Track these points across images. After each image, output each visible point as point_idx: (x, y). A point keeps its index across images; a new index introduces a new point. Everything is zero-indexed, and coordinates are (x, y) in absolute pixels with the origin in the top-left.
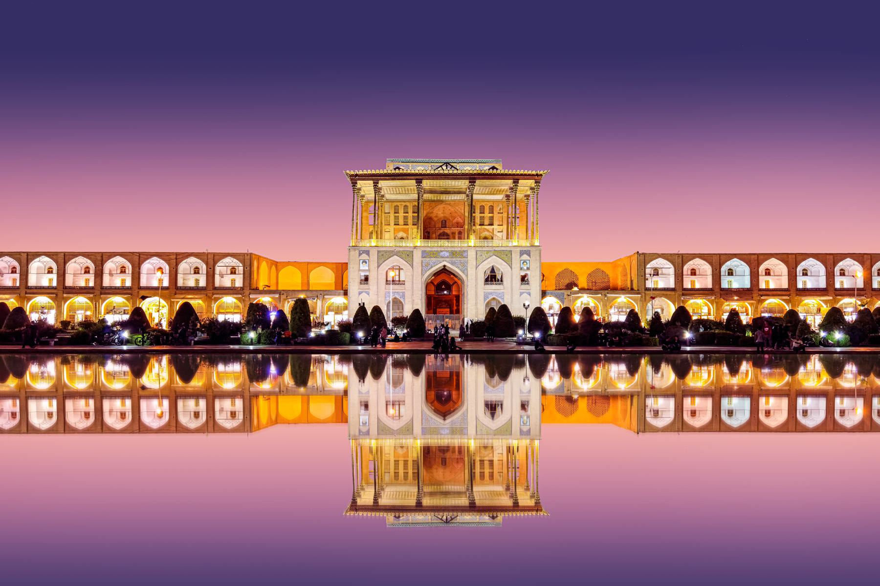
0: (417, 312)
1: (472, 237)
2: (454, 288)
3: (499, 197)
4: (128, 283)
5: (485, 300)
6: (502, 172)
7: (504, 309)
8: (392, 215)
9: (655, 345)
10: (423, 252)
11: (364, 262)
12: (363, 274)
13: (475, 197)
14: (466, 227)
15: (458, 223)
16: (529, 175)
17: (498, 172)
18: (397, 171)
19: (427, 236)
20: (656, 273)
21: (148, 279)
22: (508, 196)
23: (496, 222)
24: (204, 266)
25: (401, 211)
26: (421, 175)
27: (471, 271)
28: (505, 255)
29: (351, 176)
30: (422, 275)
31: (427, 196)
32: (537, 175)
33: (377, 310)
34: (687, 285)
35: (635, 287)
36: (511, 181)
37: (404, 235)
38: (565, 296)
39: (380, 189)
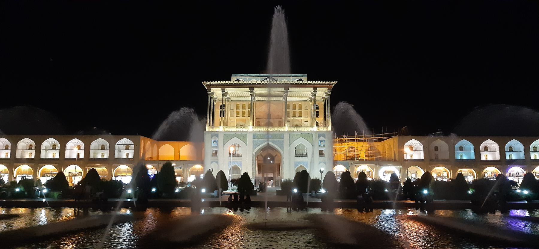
0: (246, 175)
1: (286, 125)
2: (276, 159)
3: (306, 99)
4: (57, 156)
5: (295, 167)
6: (306, 82)
8: (235, 110)
11: (215, 141)
12: (214, 149)
13: (288, 99)
15: (278, 116)
17: (304, 82)
18: (237, 82)
19: (258, 124)
21: (70, 153)
22: (310, 98)
23: (303, 115)
24: (108, 144)
26: (253, 84)
27: (286, 147)
29: (207, 85)
30: (253, 150)
35: (397, 160)
36: (312, 88)
37: (243, 124)
38: (350, 165)
39: (227, 93)
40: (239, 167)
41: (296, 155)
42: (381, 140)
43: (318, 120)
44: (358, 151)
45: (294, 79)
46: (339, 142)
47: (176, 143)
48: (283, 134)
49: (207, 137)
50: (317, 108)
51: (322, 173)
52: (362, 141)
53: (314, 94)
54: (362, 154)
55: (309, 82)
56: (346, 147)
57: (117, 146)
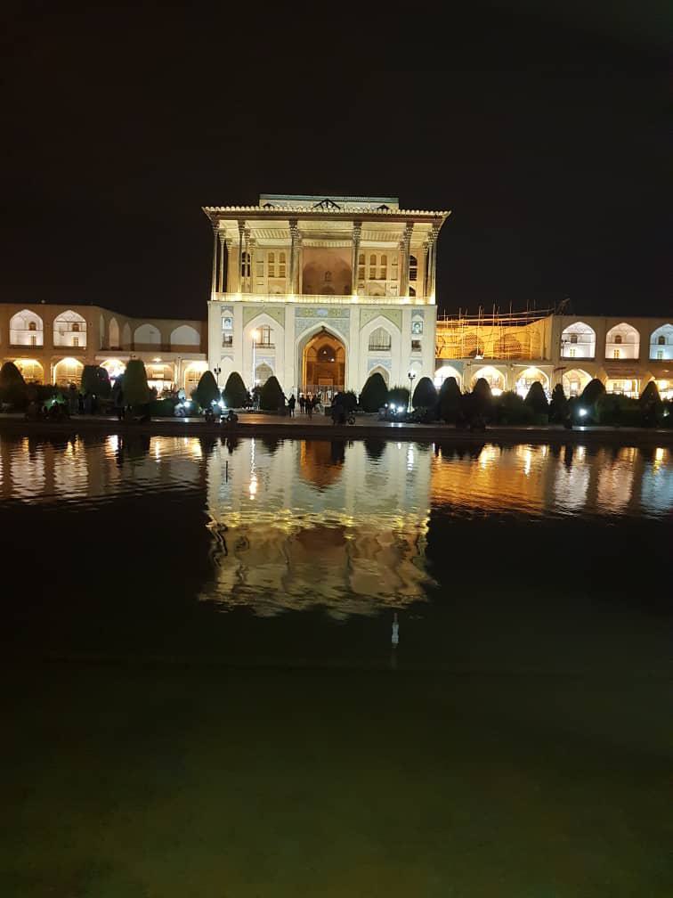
2: (339, 354)
3: (394, 245)
6: (394, 212)
8: (266, 264)
9: (543, 425)
10: (298, 310)
11: (227, 319)
12: (227, 335)
13: (362, 244)
17: (389, 212)
18: (267, 209)
19: (307, 289)
20: (574, 339)
22: (402, 243)
23: (389, 276)
24: (41, 321)
25: (277, 260)
26: (295, 214)
27: (353, 333)
28: (394, 314)
30: (296, 337)
31: (306, 242)
32: (436, 217)
33: (235, 379)
35: (548, 358)
37: (280, 290)
38: (465, 366)
39: (247, 232)
40: (271, 367)
41: (372, 348)
42: (522, 324)
43: (412, 284)
46: (449, 327)
47: (165, 323)
49: (213, 311)
51: (412, 379)
52: (490, 324)
53: (407, 235)
54: (489, 350)
56: (462, 336)
57: (57, 326)
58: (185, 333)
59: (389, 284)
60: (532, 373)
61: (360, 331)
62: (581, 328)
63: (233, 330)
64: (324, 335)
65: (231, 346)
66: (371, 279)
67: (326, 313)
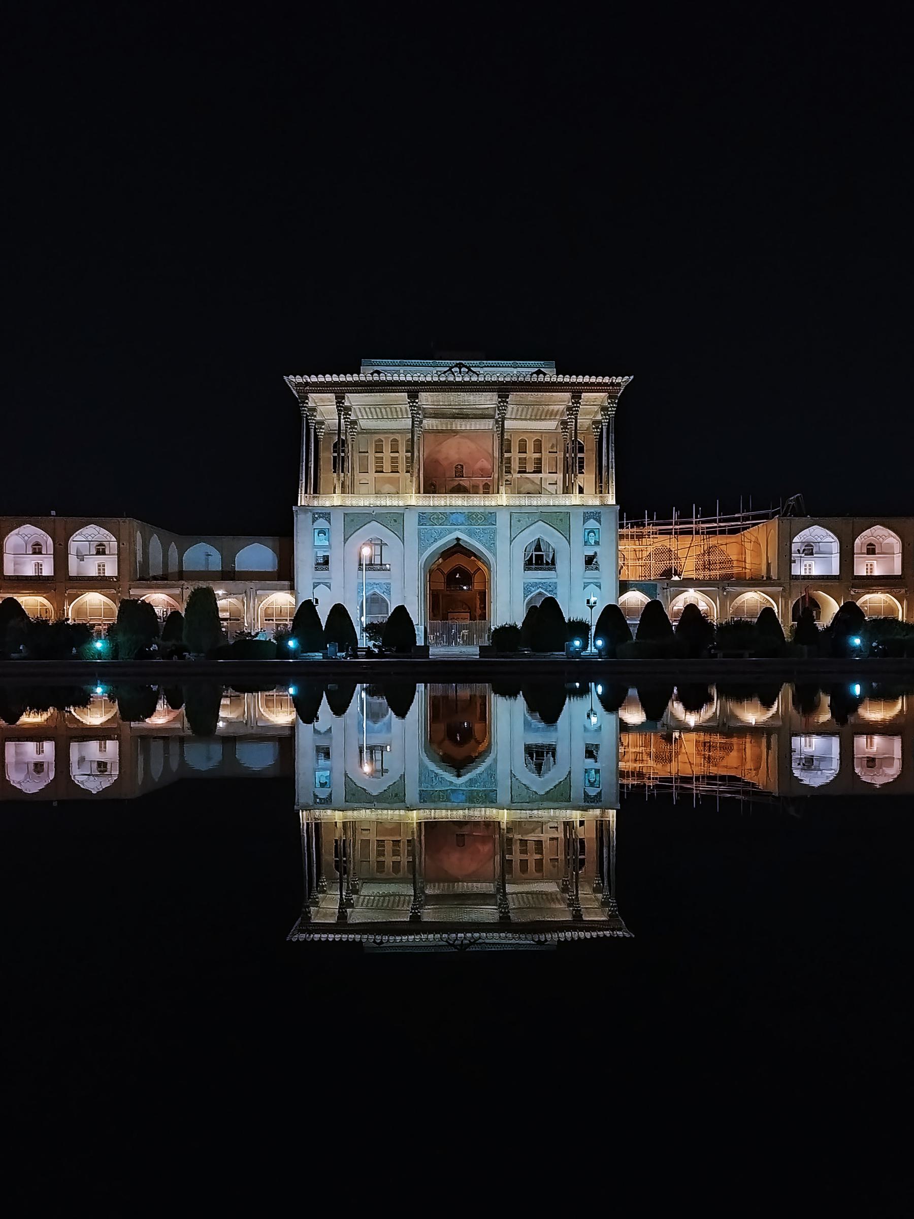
2: (477, 578)
3: (551, 425)
7: (551, 605)
11: (322, 531)
12: (321, 554)
13: (507, 424)
14: (496, 476)
15: (482, 470)
16: (599, 384)
17: (547, 379)
18: (376, 378)
20: (809, 550)
22: (564, 423)
23: (545, 467)
25: (387, 448)
27: (502, 545)
28: (559, 519)
31: (428, 423)
32: (612, 384)
33: (339, 612)
34: (861, 570)
35: (774, 576)
36: (568, 395)
40: (385, 597)
43: (581, 480)
44: (677, 558)
45: (523, 371)
47: (227, 540)
48: (493, 515)
50: (581, 450)
51: (591, 607)
52: (689, 532)
53: (572, 410)
54: (689, 569)
55: (560, 379)
58: (256, 555)
59: (546, 479)
60: (753, 598)
61: (511, 542)
62: (817, 533)
63: (330, 546)
64: (456, 553)
65: (328, 570)
66: (519, 472)
67: (461, 519)
